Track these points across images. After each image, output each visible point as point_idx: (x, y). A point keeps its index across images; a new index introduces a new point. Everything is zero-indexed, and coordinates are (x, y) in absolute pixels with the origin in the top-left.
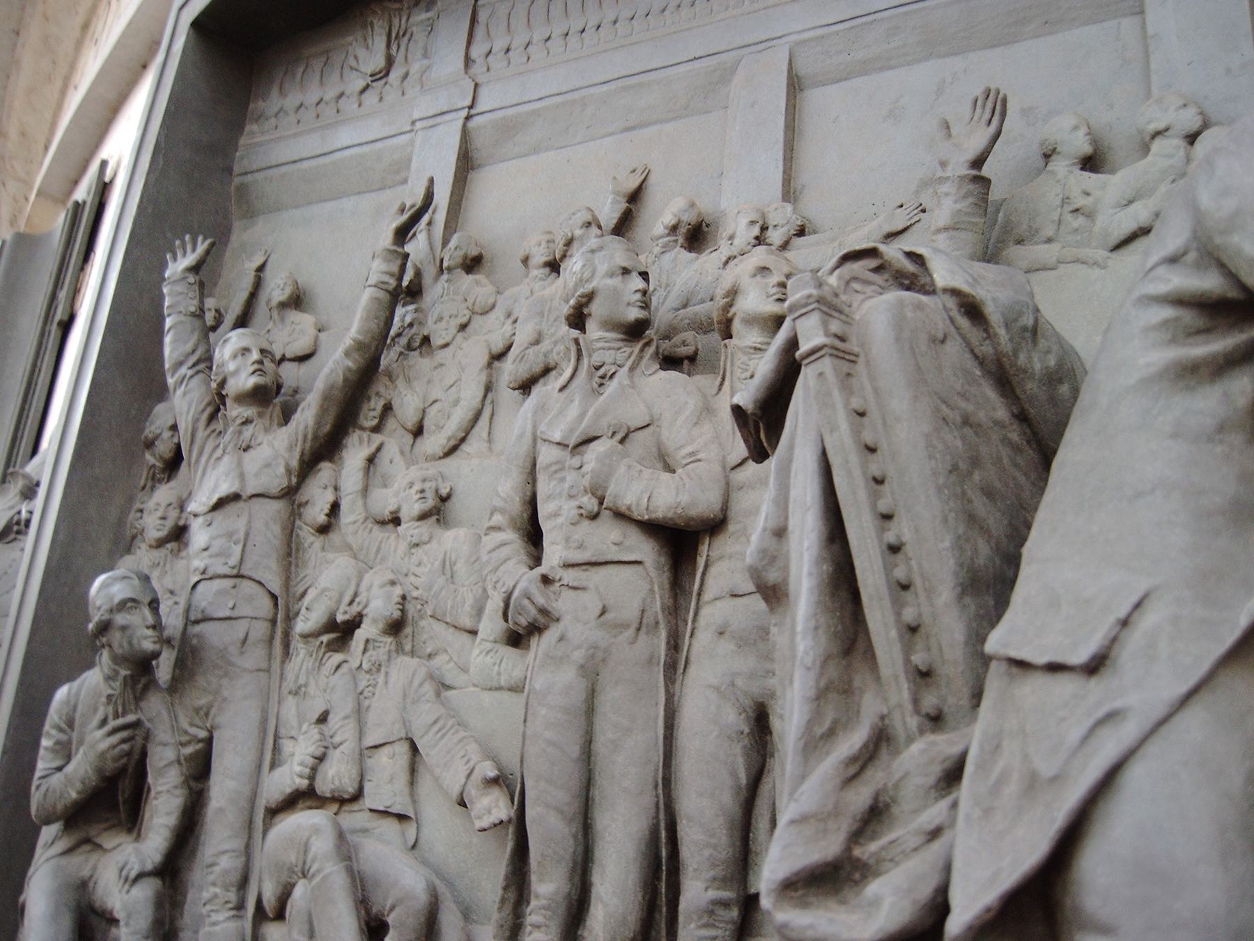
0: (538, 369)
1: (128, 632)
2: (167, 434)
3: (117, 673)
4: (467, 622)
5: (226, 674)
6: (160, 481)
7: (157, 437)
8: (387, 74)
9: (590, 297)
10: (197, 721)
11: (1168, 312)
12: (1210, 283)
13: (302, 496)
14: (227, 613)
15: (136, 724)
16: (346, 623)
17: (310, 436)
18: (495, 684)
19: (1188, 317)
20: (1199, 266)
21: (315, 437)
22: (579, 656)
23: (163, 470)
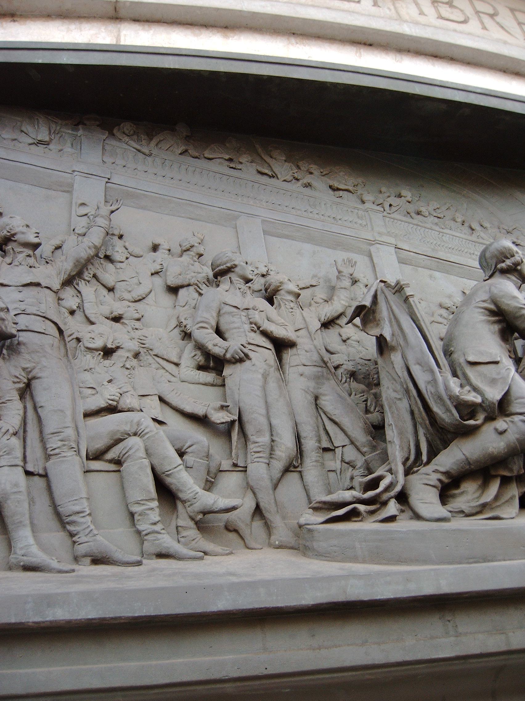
0: (185, 283)
1: (7, 322)
4: (175, 360)
5: (45, 356)
8: (48, 144)
9: (236, 266)
10: (23, 374)
11: (483, 310)
12: (492, 307)
14: (43, 331)
16: (112, 349)
17: (68, 273)
18: (197, 382)
19: (487, 312)
20: (490, 303)
21: (69, 275)
22: (261, 371)
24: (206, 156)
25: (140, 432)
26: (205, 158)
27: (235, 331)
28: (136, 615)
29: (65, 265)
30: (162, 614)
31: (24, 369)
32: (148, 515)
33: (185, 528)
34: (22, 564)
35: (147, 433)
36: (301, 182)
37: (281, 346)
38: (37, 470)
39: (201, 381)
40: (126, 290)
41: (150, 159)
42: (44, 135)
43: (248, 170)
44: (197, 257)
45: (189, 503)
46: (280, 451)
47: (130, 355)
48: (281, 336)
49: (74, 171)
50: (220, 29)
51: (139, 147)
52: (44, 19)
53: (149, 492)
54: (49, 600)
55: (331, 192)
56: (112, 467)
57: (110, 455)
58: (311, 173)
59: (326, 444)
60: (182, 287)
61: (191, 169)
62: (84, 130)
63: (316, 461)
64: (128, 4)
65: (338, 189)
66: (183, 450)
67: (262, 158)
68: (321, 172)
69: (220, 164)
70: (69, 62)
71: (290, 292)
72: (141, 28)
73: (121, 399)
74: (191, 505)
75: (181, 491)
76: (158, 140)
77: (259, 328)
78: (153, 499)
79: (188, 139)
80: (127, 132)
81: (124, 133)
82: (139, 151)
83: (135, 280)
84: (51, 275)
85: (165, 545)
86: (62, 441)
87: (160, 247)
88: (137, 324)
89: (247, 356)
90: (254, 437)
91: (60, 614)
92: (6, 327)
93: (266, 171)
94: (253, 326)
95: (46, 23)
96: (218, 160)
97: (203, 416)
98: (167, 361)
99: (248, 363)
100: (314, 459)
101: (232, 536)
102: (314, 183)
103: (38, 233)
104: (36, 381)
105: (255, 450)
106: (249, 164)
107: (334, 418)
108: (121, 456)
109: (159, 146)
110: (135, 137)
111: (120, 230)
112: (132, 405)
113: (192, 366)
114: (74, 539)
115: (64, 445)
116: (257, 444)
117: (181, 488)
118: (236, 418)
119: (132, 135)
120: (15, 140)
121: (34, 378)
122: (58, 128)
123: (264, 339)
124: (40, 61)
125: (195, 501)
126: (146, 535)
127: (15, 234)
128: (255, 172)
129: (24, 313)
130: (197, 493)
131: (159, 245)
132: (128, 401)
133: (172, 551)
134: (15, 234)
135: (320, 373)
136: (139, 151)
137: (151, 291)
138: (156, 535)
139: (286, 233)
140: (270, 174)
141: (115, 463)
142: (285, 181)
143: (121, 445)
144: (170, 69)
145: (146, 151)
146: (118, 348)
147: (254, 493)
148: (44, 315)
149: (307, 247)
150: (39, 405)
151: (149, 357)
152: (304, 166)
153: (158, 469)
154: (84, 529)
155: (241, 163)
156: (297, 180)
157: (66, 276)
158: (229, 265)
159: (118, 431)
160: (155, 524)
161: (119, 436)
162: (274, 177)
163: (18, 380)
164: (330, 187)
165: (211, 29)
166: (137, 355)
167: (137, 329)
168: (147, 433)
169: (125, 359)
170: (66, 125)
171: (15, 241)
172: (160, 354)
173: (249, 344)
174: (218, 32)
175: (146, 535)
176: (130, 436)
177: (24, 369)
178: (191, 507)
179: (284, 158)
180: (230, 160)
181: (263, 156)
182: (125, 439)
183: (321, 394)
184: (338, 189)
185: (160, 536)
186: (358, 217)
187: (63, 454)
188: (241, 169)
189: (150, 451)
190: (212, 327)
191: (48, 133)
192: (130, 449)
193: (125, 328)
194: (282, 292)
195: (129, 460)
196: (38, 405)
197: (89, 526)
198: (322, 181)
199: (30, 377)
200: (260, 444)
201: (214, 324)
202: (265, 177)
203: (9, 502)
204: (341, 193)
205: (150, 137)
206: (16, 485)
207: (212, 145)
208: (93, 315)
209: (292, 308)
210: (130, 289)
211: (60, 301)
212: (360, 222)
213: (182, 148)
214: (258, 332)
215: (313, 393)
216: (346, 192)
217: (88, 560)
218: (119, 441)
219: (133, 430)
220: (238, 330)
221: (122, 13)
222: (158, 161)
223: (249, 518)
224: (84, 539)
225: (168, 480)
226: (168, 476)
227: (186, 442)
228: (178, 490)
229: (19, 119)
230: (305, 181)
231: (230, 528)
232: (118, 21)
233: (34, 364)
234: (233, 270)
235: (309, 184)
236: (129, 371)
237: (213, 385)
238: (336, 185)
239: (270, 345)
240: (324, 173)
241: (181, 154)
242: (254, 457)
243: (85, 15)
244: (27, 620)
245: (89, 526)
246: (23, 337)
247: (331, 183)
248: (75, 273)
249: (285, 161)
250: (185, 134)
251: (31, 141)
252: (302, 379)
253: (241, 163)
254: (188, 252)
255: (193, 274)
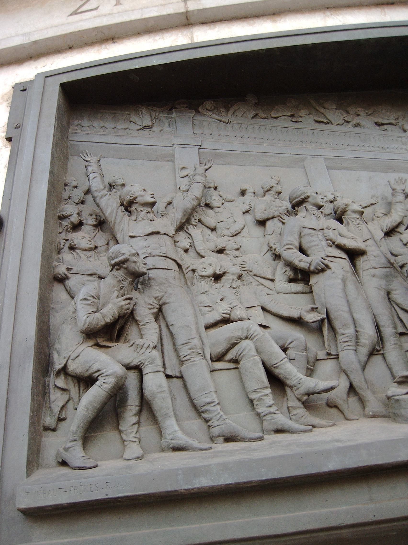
0: (271, 216)
1: (138, 264)
2: (75, 215)
3: (126, 279)
4: (270, 277)
5: (170, 286)
6: (69, 232)
7: (71, 215)
8: (151, 128)
9: (308, 197)
13: (177, 238)
14: (166, 267)
15: (130, 299)
17: (179, 221)
21: (180, 222)
22: (340, 277)
23: (71, 228)
24: (273, 116)
25: (250, 336)
26: (272, 117)
27: (314, 248)
28: (264, 479)
29: (176, 215)
30: (284, 476)
31: (155, 298)
32: (264, 400)
33: (295, 408)
34: (171, 446)
35: (256, 336)
36: (351, 123)
37: (354, 255)
38: (174, 374)
39: (293, 290)
40: (225, 228)
41: (229, 126)
42: (147, 122)
43: (308, 121)
44: (277, 195)
45: (295, 388)
46: (364, 339)
47: (235, 277)
48: (353, 247)
49: (173, 144)
50: (269, 17)
51: (220, 118)
52: (135, 37)
53: (263, 382)
54: (195, 472)
55: (377, 127)
56: (232, 365)
57: (229, 356)
58: (358, 115)
59: (401, 329)
60: (268, 219)
61: (262, 128)
62: (176, 112)
63: (395, 344)
64: (196, 12)
65: (383, 124)
66: (285, 347)
67: (317, 110)
68: (367, 113)
69: (284, 120)
70: (158, 64)
71: (355, 212)
72: (208, 28)
73: (232, 312)
74: (297, 389)
75: (288, 379)
76: (234, 110)
77: (334, 243)
78: (266, 387)
79: (256, 105)
80: (209, 108)
81: (207, 109)
82: (220, 121)
83: (231, 220)
84: (167, 225)
85: (280, 422)
86: (191, 349)
87: (247, 191)
88: (237, 253)
89: (327, 266)
90: (341, 330)
91: (204, 482)
92: (138, 267)
93: (322, 120)
94: (329, 242)
95: (138, 39)
96: (283, 118)
97: (298, 318)
98: (264, 278)
99: (328, 271)
100: (393, 342)
101: (333, 411)
102: (362, 123)
103: (153, 194)
104: (166, 306)
105: (343, 340)
106: (307, 116)
107: (405, 307)
108: (238, 356)
109: (236, 114)
110: (216, 111)
111: (214, 183)
112: (241, 316)
113: (284, 280)
114: (209, 424)
115: (193, 352)
116: (344, 336)
117: (287, 376)
118: (325, 316)
119: (213, 110)
120: (127, 128)
121: (164, 304)
122: (157, 114)
123: (339, 251)
124: (137, 67)
125: (300, 385)
126: (264, 416)
127: (136, 198)
128: (313, 122)
129: (150, 255)
130: (301, 379)
131: (246, 190)
132: (238, 313)
133: (286, 427)
134: (136, 198)
135: (389, 273)
136: (220, 121)
137: (244, 226)
138: (272, 415)
139: (345, 165)
140: (325, 121)
141: (233, 362)
142: (338, 125)
143: (236, 348)
144: (235, 53)
145: (226, 120)
146: (225, 273)
147: (347, 375)
148: (165, 255)
149: (364, 174)
150: (171, 324)
151: (250, 277)
152: (352, 110)
153: (268, 363)
154: (216, 415)
155: (301, 117)
156: (348, 122)
157: (178, 224)
158: (303, 197)
159: (233, 336)
160: (270, 406)
161: (234, 341)
162: (328, 123)
163: (152, 307)
164: (376, 123)
165: (262, 18)
166: (240, 277)
167: (237, 257)
168: (256, 336)
169: (231, 281)
170: (163, 111)
171: (137, 203)
172: (258, 274)
173: (328, 256)
174: (268, 19)
175: (264, 416)
176: (243, 340)
177: (155, 298)
178: (298, 391)
179: (335, 107)
180: (292, 116)
181: (318, 109)
182: (239, 343)
183: (392, 290)
184: (383, 124)
185: (275, 416)
186: (403, 144)
187: (193, 359)
188: (301, 122)
189: (260, 350)
190: (296, 247)
191: (150, 119)
192: (244, 350)
193: (228, 257)
194: (349, 212)
195: (244, 359)
196: (170, 324)
197: (219, 413)
198: (368, 120)
199: (161, 303)
200: (347, 335)
201: (297, 244)
202: (321, 125)
203: (156, 399)
204: (385, 127)
205: (227, 109)
206: (160, 386)
207: (276, 107)
208: (203, 251)
209: (358, 224)
210: (228, 227)
211: (176, 244)
212: (404, 147)
213: (253, 113)
214: (333, 246)
215: (385, 289)
216: (389, 126)
217: (222, 439)
218: (234, 345)
219: (245, 335)
220: (317, 247)
221: (193, 19)
222: (236, 126)
223: (345, 396)
224: (216, 423)
225: (277, 371)
226: (276, 368)
227: (287, 340)
228: (285, 378)
229: (128, 113)
230: (354, 122)
231: (331, 405)
232: (190, 26)
233: (163, 293)
234: (306, 200)
235: (358, 124)
236: (235, 290)
237: (303, 293)
238: (380, 121)
239: (344, 256)
240: (369, 113)
241: (252, 118)
242: (343, 346)
243: (165, 27)
244: (180, 488)
245: (219, 413)
246: (152, 274)
247: (376, 120)
248: (184, 220)
249: (336, 109)
250: (253, 102)
251: (139, 127)
252: (374, 279)
253: (301, 117)
254: (269, 192)
255: (276, 209)
